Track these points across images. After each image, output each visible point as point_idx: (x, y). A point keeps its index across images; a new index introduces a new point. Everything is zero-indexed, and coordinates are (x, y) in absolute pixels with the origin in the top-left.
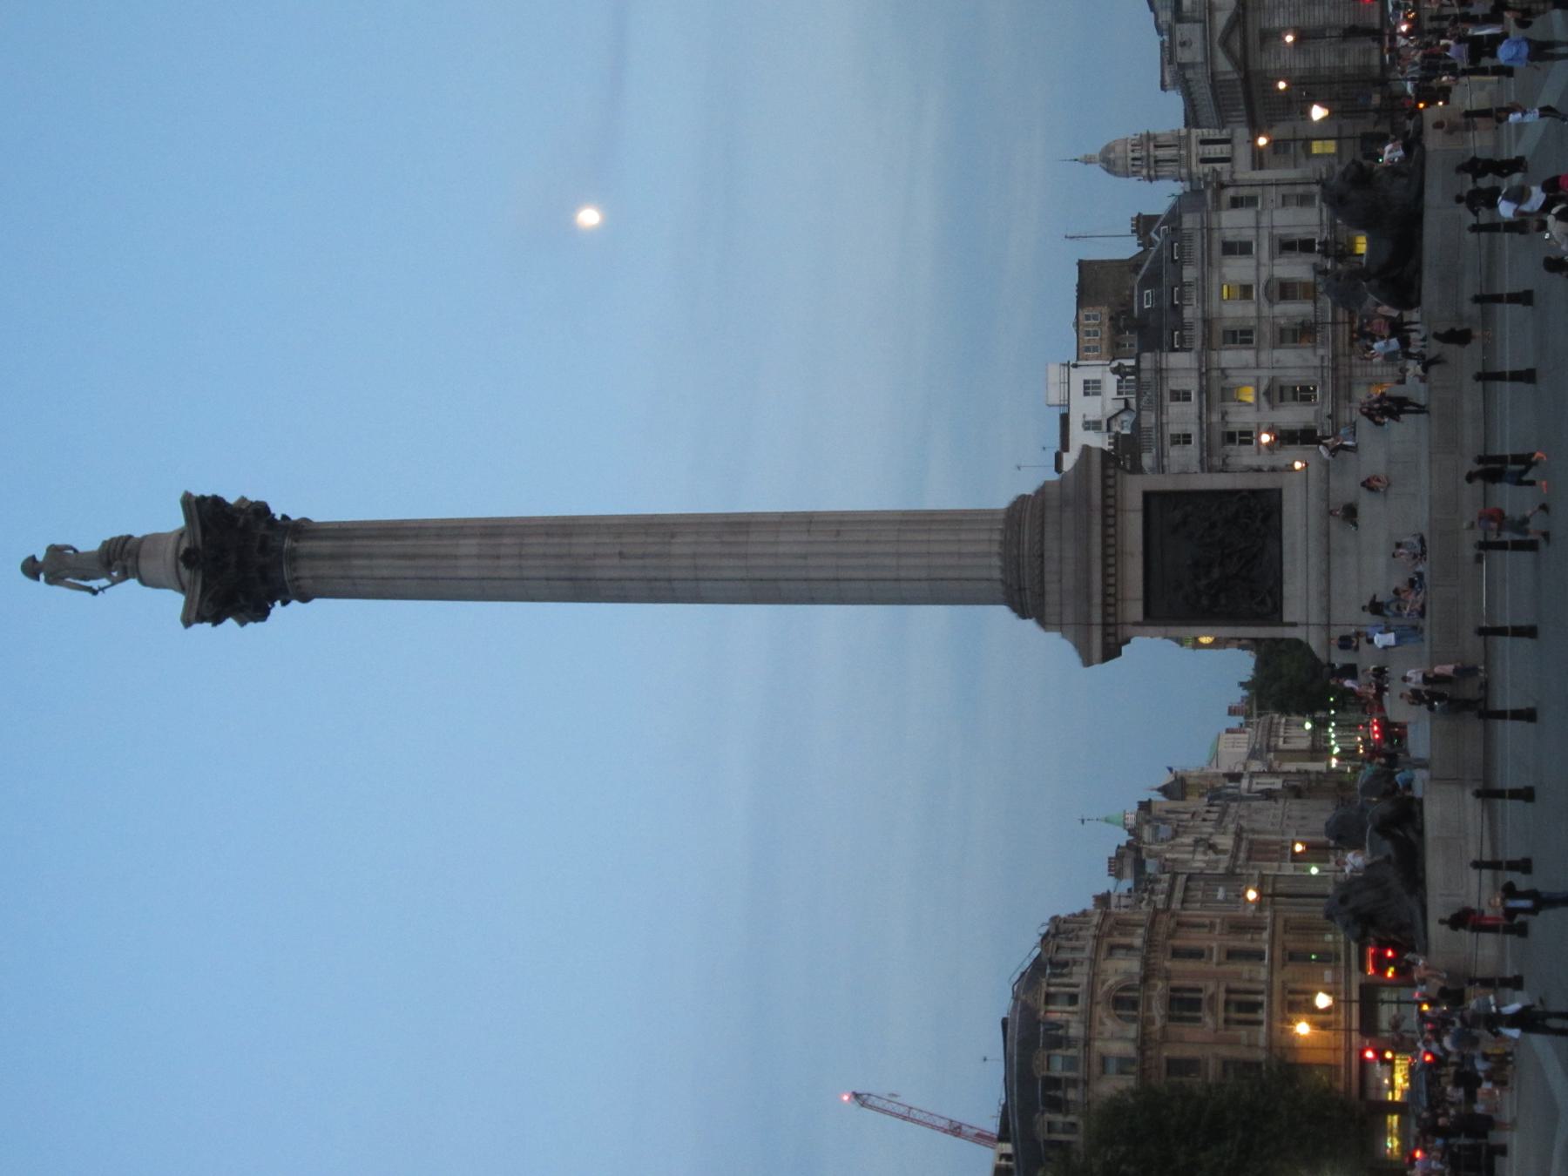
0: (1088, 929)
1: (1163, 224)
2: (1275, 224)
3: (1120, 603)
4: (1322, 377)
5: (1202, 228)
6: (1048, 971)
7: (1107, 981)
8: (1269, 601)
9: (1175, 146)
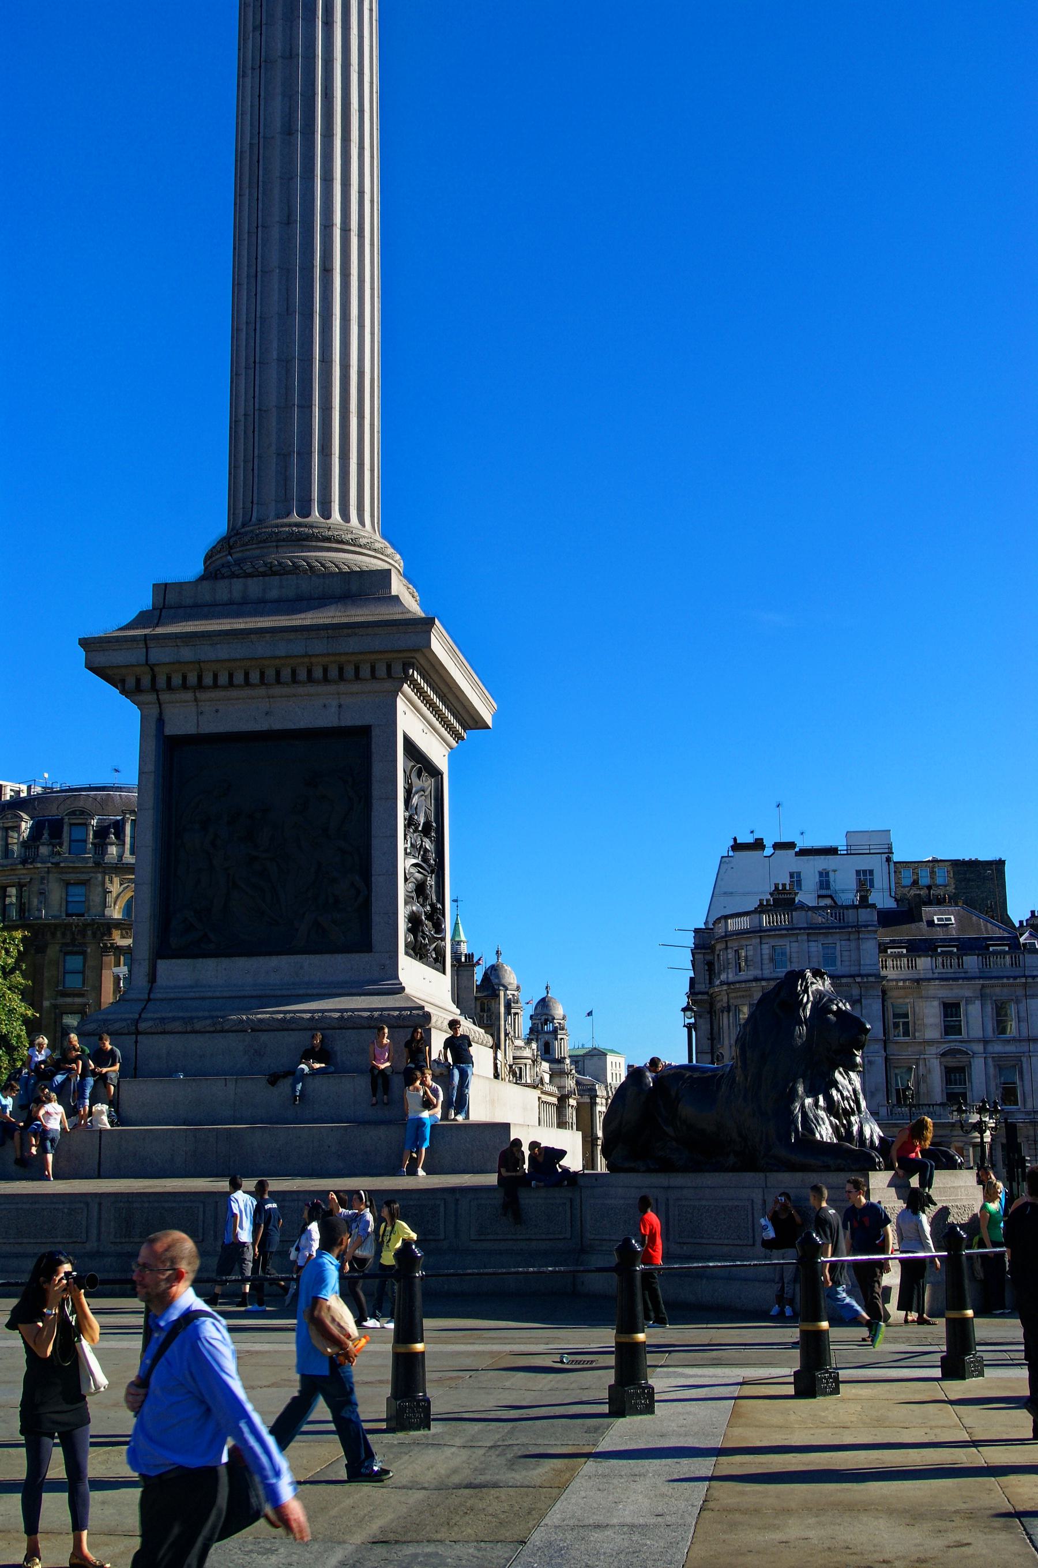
3: (189, 696)
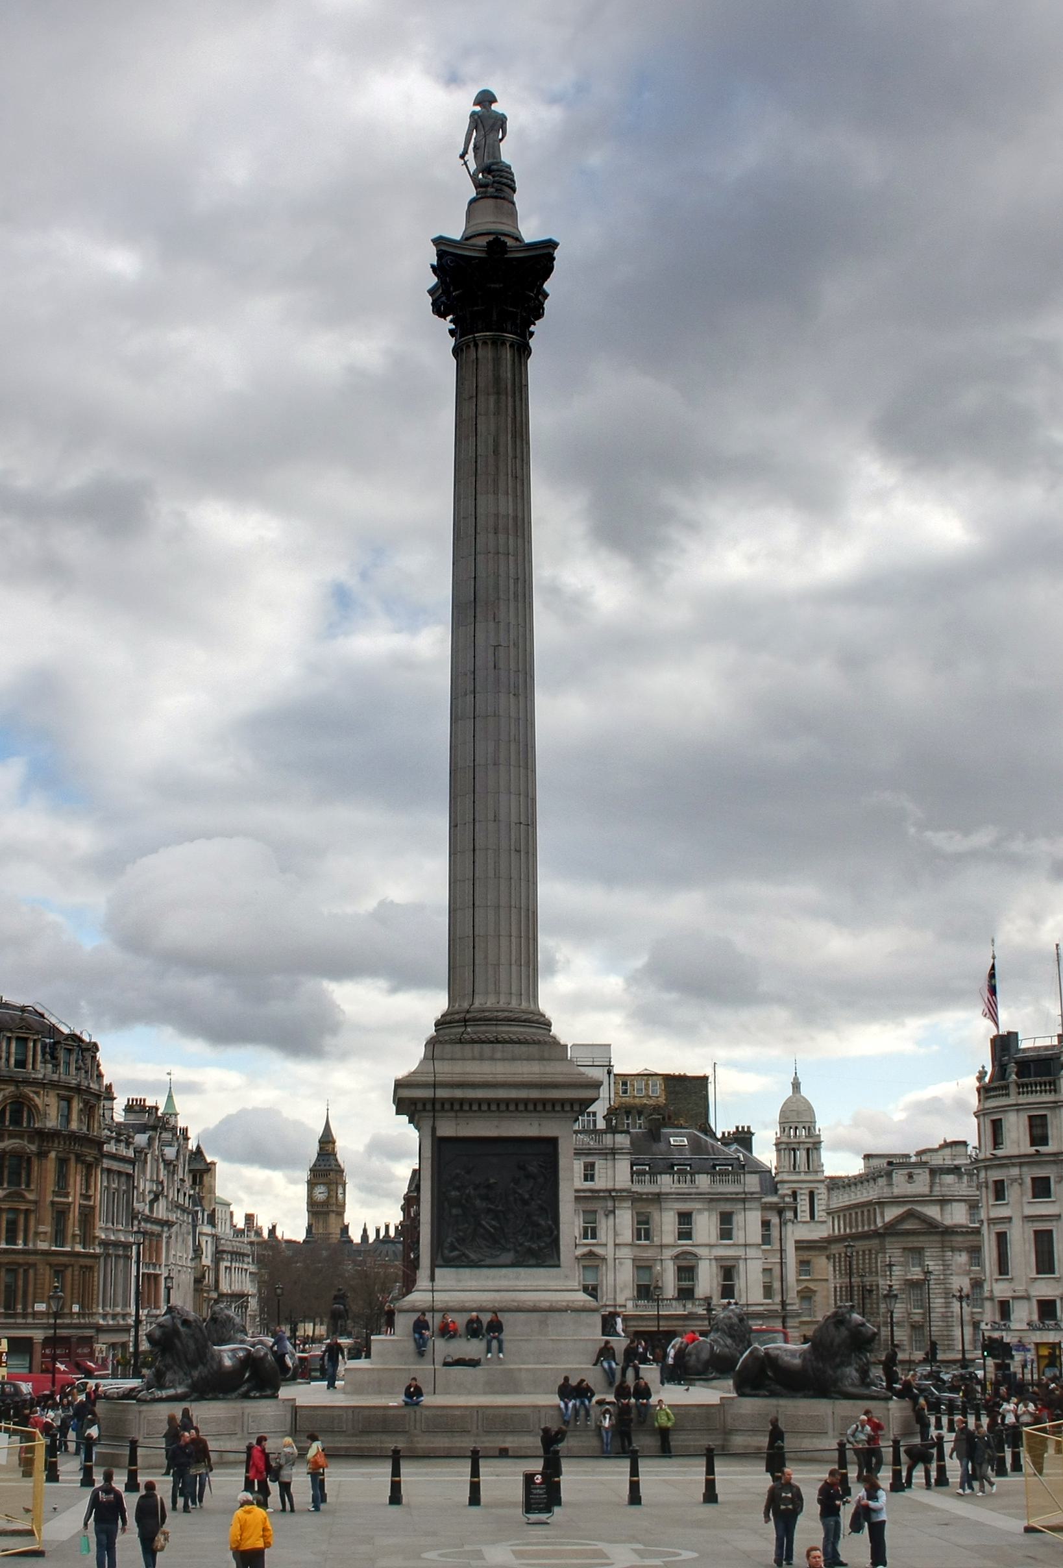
0: (86, 1078)
1: (744, 1155)
2: (748, 1261)
3: (453, 1114)
4: (607, 1306)
5: (745, 1193)
6: (48, 1041)
7: (39, 1097)
8: (456, 1253)
9: (808, 1168)
